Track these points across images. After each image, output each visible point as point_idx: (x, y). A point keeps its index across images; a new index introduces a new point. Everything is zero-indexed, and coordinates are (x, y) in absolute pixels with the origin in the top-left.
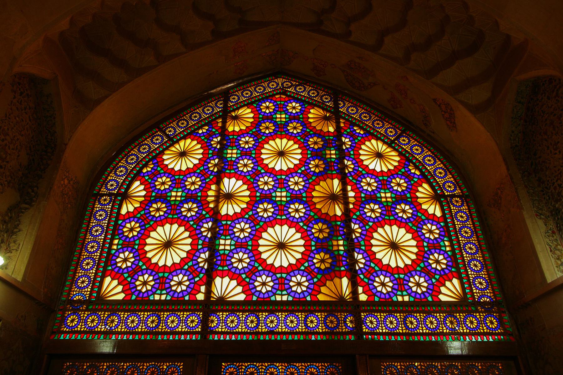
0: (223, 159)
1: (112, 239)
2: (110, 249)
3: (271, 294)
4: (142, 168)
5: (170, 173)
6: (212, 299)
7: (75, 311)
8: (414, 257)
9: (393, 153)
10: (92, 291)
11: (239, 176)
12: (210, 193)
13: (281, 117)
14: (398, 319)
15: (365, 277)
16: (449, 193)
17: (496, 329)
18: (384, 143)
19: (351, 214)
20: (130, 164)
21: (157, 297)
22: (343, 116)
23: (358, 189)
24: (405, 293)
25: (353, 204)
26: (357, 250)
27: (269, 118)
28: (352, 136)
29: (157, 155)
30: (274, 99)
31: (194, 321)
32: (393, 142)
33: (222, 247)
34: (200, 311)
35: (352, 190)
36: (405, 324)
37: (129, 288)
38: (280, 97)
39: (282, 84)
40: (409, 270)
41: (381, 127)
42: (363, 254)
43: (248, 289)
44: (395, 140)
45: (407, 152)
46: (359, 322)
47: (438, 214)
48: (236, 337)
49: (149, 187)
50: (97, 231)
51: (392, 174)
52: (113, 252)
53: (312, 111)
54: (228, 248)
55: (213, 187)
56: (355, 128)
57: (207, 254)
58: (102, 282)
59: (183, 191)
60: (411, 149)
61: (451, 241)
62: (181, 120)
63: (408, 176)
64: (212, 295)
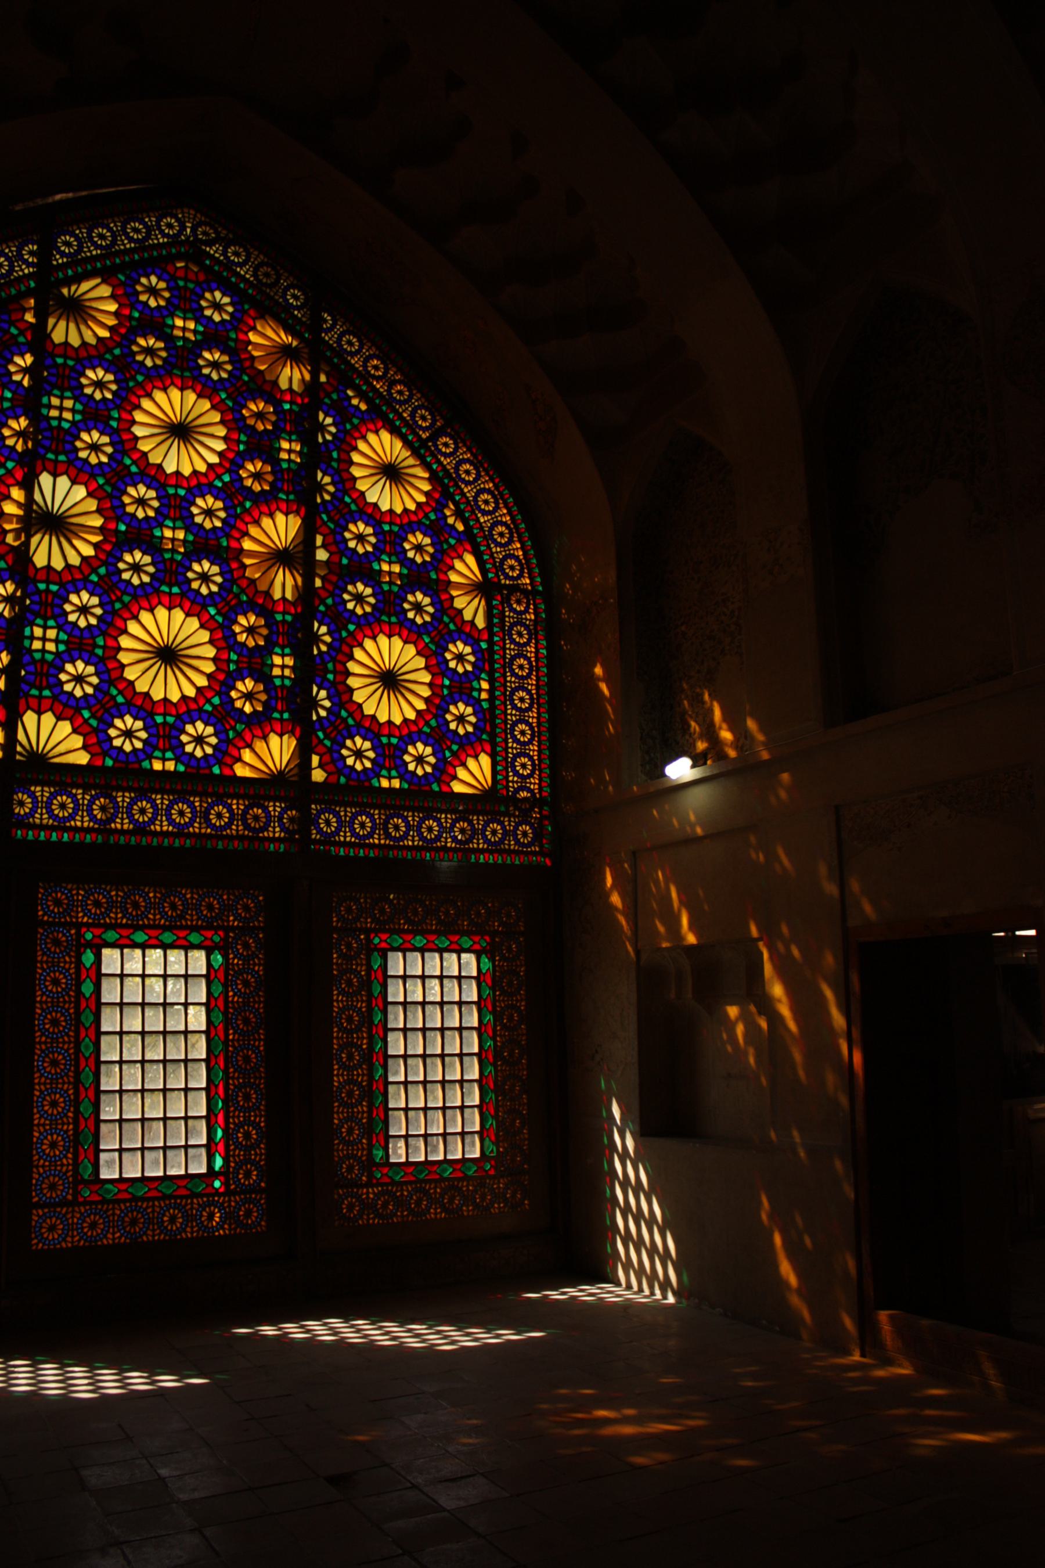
0: (38, 420)
3: (141, 755)
8: (421, 706)
9: (420, 472)
11: (80, 472)
16: (507, 582)
17: (530, 844)
18: (407, 444)
19: (317, 602)
22: (328, 354)
23: (337, 544)
28: (342, 412)
30: (170, 268)
32: (424, 443)
33: (37, 645)
35: (324, 546)
39: (194, 230)
40: (409, 733)
41: (406, 402)
44: (428, 439)
46: (307, 821)
51: (409, 522)
54: (51, 647)
55: (17, 493)
56: (350, 393)
60: (457, 469)
61: (491, 681)
63: (438, 530)
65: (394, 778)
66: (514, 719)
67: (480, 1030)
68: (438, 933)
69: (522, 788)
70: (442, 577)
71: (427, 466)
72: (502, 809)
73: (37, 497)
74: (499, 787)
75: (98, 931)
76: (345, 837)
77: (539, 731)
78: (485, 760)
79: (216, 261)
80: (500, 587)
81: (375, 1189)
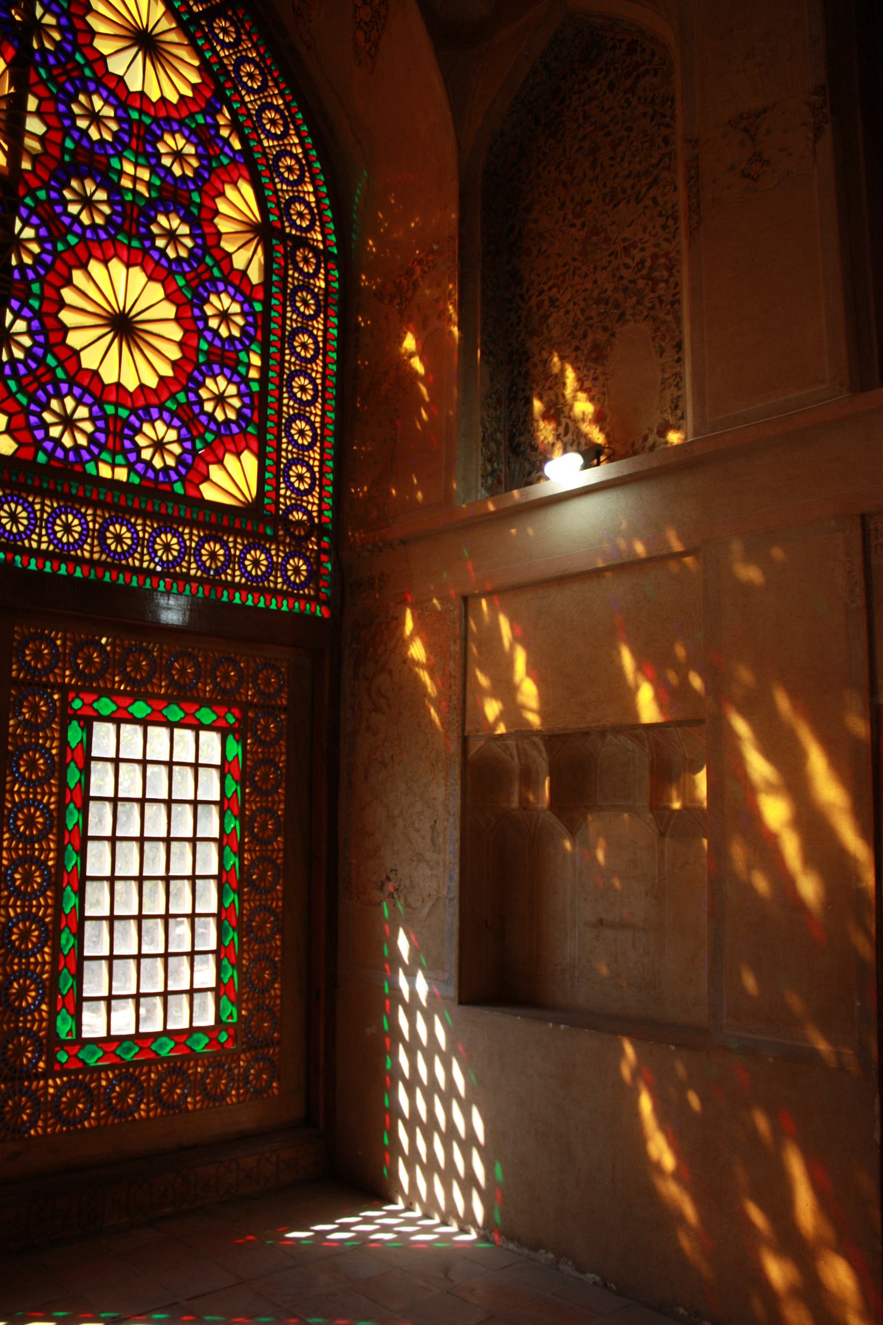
8: (167, 371)
14: (87, 523)
15: (21, 389)
16: (294, 232)
24: (119, 459)
26: (15, 304)
35: (39, 113)
36: (102, 539)
42: (29, 321)
47: (255, 276)
61: (265, 356)
65: (120, 466)
66: (291, 412)
67: (222, 841)
68: (169, 700)
70: (207, 202)
71: (198, 52)
72: (269, 531)
74: (266, 501)
76: (39, 542)
77: (322, 435)
78: (250, 461)
80: (285, 238)
81: (58, 1081)
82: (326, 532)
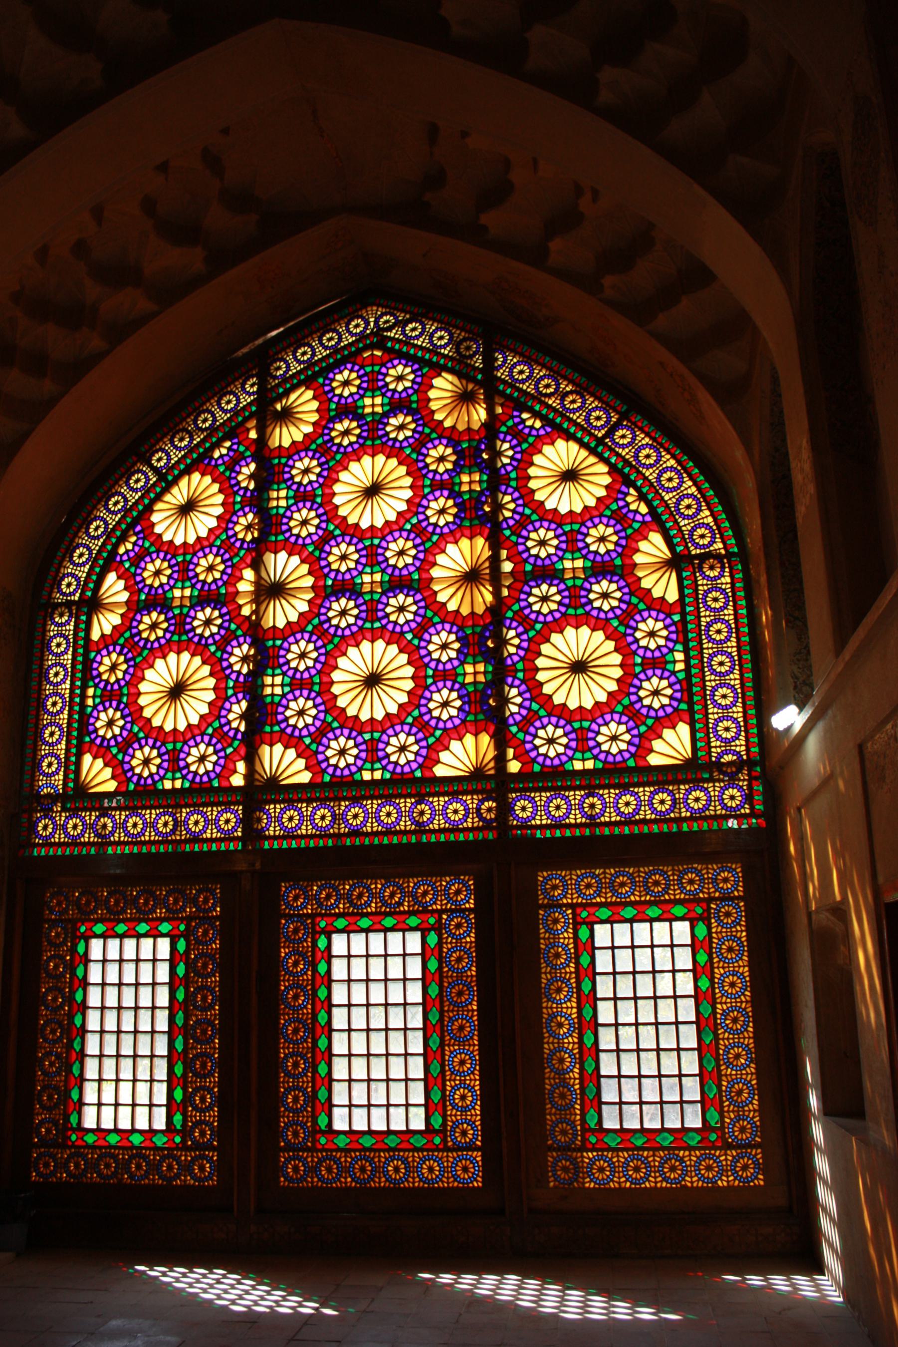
1: (84, 688)
2: (83, 705)
4: (116, 546)
5: (168, 550)
6: (257, 783)
7: (47, 813)
10: (66, 780)
11: (294, 547)
12: (243, 586)
13: (372, 404)
20: (94, 538)
21: (168, 785)
25: (508, 587)
27: (349, 410)
28: (518, 434)
29: (141, 513)
31: (229, 819)
32: (600, 441)
34: (237, 803)
37: (121, 772)
38: (372, 355)
39: (376, 322)
43: (314, 763)
44: (605, 436)
45: (627, 463)
46: (505, 809)
47: (672, 596)
48: (298, 844)
49: (133, 583)
50: (56, 674)
52: (89, 710)
53: (437, 382)
57: (244, 704)
58: (78, 764)
59: (193, 586)
60: (636, 456)
61: (686, 651)
62: (177, 433)
63: (621, 519)
64: (257, 777)
69: (726, 752)
71: (606, 461)
72: (706, 776)
73: (264, 574)
75: (330, 919)
79: (398, 341)
82: (755, 764)
